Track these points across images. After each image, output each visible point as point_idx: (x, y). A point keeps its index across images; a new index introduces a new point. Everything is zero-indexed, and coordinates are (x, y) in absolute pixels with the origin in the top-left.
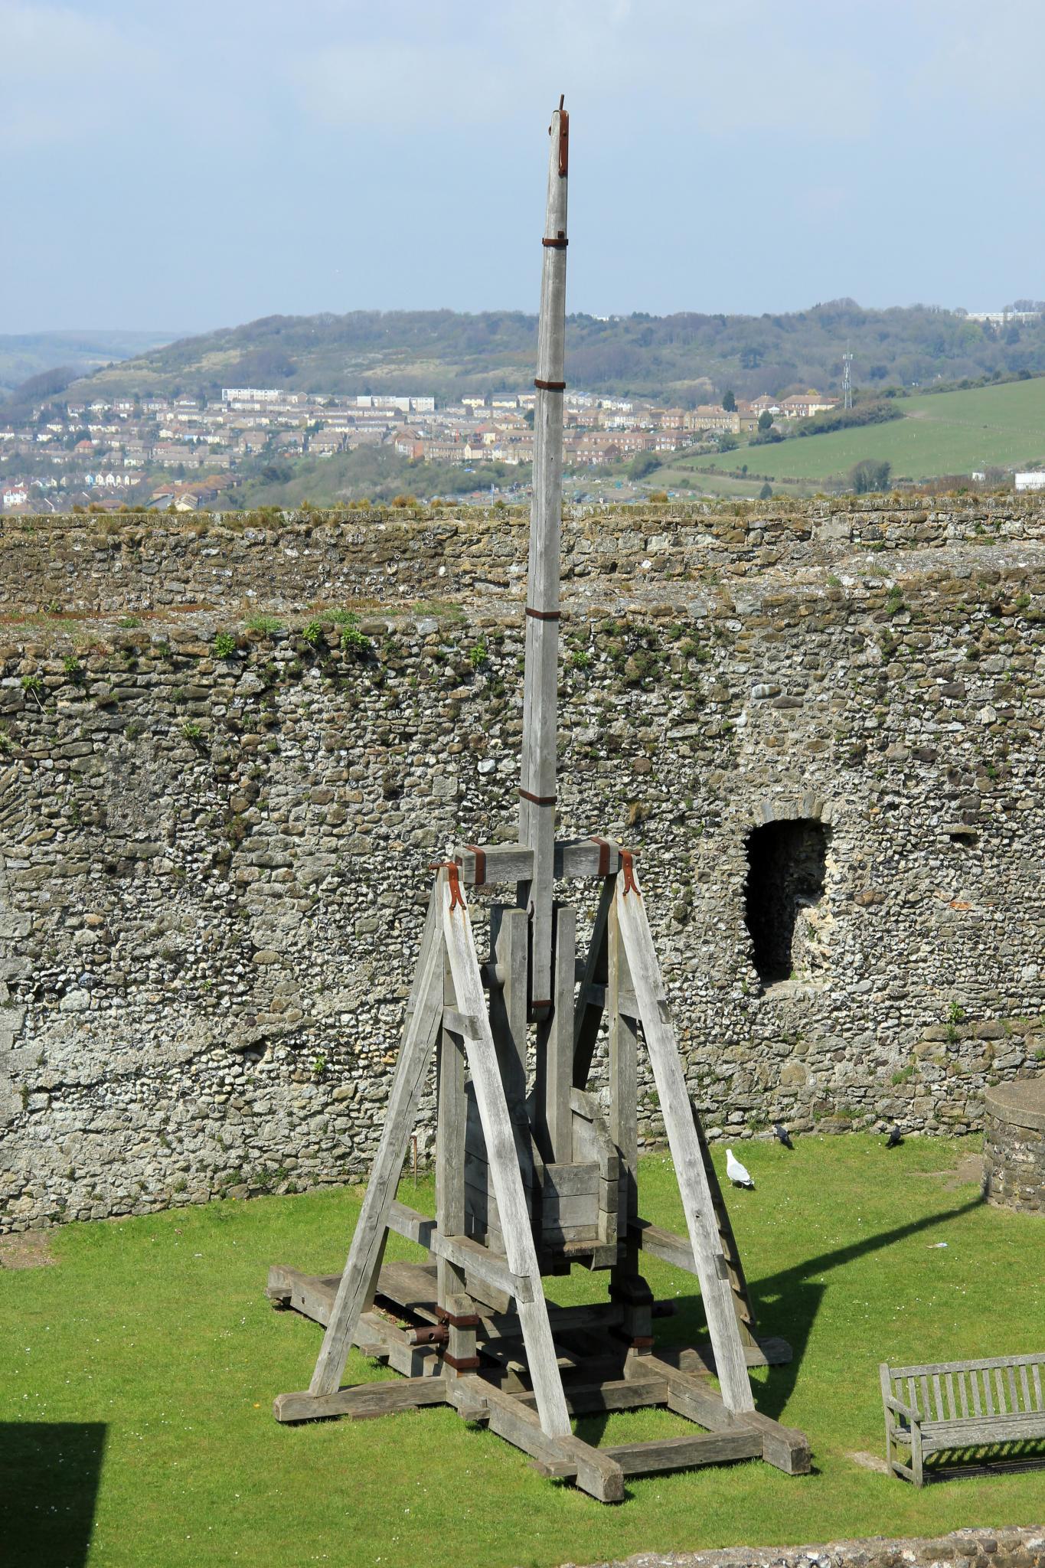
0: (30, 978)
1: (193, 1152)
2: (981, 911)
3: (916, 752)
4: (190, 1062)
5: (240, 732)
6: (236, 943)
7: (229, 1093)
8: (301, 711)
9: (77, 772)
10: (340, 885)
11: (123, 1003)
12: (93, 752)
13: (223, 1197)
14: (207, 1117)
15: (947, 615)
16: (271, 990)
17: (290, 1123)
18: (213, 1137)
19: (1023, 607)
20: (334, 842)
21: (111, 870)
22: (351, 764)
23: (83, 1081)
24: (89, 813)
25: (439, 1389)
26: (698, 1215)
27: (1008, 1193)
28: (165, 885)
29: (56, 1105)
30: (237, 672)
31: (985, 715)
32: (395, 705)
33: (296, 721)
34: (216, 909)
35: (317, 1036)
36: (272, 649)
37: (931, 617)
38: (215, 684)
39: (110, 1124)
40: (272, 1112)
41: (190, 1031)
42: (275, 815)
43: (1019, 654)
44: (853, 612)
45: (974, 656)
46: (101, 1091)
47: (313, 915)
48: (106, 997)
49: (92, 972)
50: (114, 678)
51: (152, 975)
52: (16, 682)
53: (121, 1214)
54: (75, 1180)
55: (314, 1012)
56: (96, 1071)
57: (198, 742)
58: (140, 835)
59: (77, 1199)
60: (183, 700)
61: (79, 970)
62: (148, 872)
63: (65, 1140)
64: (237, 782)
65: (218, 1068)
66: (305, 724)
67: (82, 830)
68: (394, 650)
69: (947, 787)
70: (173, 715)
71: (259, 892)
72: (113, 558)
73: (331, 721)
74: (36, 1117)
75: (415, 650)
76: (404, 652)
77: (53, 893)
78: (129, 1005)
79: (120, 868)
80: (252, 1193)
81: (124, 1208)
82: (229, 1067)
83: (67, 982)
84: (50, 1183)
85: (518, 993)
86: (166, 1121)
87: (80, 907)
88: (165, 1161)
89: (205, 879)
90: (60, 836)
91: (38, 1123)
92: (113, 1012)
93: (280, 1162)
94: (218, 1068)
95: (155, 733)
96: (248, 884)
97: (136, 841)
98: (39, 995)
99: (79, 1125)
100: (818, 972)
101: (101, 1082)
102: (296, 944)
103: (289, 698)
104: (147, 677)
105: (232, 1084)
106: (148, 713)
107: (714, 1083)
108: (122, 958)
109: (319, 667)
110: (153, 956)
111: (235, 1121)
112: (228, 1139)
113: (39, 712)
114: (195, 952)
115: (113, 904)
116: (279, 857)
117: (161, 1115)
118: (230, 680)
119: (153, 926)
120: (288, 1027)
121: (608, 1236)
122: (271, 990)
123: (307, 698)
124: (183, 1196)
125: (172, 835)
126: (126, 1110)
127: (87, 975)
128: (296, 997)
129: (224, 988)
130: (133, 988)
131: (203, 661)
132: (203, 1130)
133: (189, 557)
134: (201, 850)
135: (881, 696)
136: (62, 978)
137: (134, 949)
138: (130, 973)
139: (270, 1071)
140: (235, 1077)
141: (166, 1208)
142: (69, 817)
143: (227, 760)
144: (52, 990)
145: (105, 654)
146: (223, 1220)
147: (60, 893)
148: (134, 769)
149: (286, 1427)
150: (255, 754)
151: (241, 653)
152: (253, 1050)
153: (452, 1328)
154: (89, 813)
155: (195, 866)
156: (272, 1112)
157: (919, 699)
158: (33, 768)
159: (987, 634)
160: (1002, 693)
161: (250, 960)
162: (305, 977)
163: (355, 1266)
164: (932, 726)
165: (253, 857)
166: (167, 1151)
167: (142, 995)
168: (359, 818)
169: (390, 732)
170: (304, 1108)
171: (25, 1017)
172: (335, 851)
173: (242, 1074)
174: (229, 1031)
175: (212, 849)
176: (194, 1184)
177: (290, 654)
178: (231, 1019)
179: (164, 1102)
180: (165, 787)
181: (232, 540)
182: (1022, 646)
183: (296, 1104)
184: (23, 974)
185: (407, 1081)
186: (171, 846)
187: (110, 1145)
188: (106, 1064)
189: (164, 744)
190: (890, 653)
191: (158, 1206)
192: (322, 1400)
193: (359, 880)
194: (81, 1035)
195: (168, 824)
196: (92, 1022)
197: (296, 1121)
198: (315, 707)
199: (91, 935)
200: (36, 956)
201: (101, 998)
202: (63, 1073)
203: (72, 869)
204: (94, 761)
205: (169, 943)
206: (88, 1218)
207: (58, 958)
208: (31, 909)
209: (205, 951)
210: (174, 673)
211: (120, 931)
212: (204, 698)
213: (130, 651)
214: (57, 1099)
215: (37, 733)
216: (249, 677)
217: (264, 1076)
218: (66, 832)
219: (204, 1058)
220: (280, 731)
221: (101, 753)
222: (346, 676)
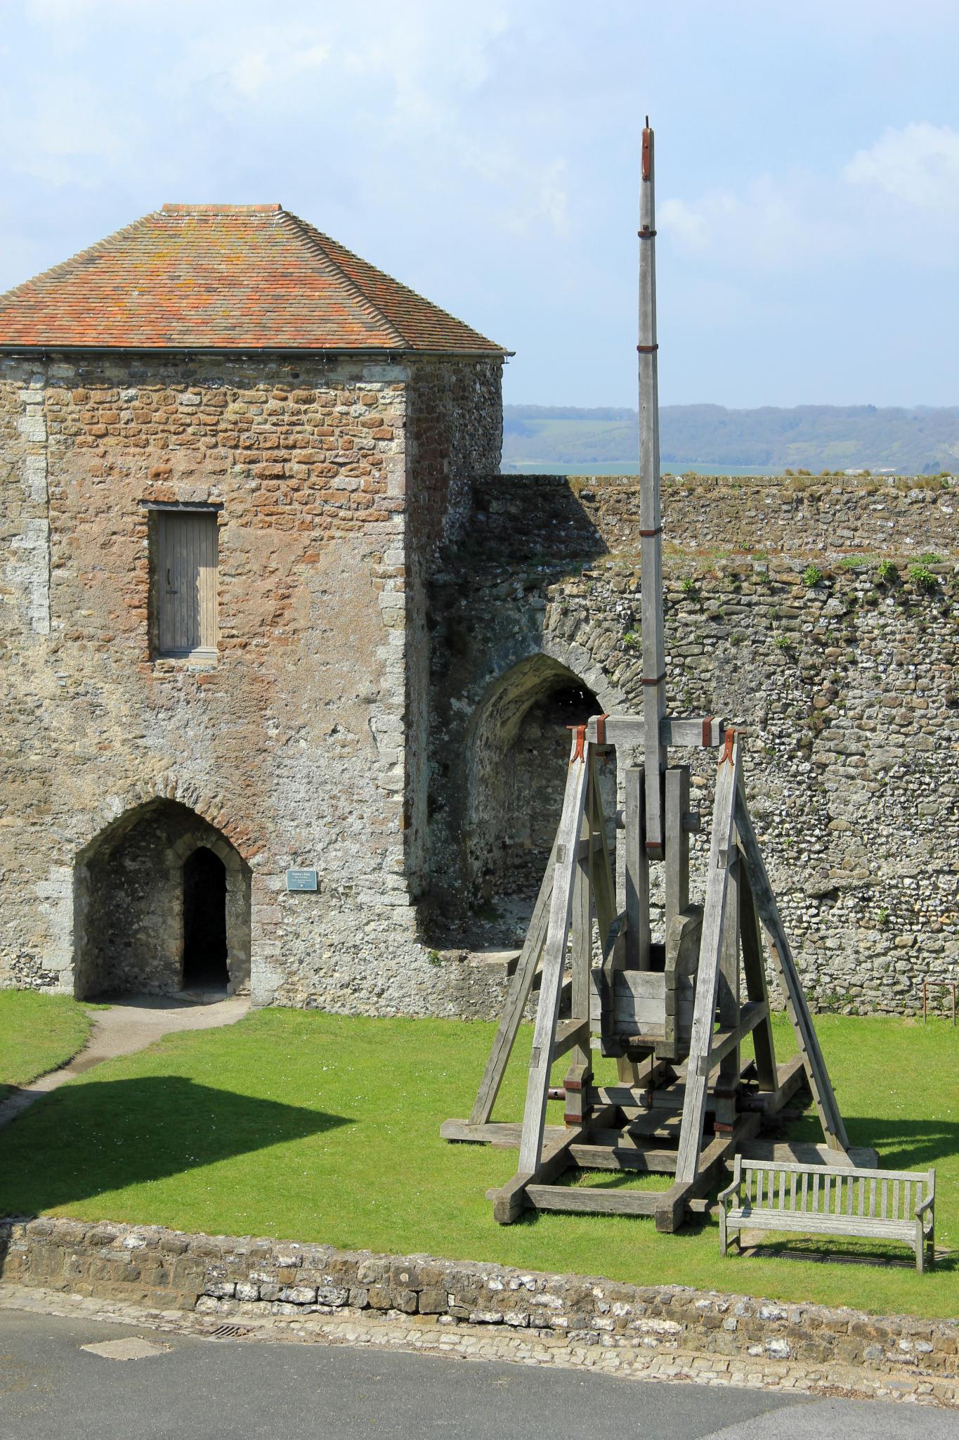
5: (825, 645)
6: (815, 811)
7: (807, 928)
8: (876, 632)
10: (905, 774)
12: (703, 653)
17: (857, 959)
20: (901, 739)
22: (917, 678)
28: (757, 760)
34: (799, 783)
36: (853, 581)
38: (805, 607)
40: (841, 948)
42: (851, 713)
47: (882, 796)
57: (787, 649)
58: (739, 720)
60: (778, 617)
64: (820, 684)
67: (692, 711)
70: (770, 628)
71: (835, 773)
72: (797, 509)
73: (903, 641)
82: (808, 908)
89: (791, 758)
93: (847, 989)
96: (826, 766)
102: (865, 817)
103: (866, 621)
104: (748, 598)
106: (748, 627)
109: (893, 597)
111: (810, 951)
114: (780, 815)
116: (853, 747)
118: (818, 604)
120: (856, 883)
123: (882, 622)
125: (764, 722)
128: (864, 860)
131: (795, 588)
133: (859, 511)
134: (789, 736)
142: (683, 701)
143: (813, 667)
145: (716, 578)
150: (836, 664)
151: (827, 583)
152: (831, 895)
155: (782, 747)
168: (924, 721)
170: (869, 949)
172: (902, 746)
173: (817, 915)
175: (796, 735)
178: (809, 870)
180: (761, 684)
181: (896, 498)
183: (862, 945)
189: (761, 650)
193: (923, 772)
195: (761, 713)
197: (862, 959)
198: (888, 629)
204: (704, 660)
205: (759, 806)
209: (788, 815)
212: (796, 617)
213: (735, 577)
216: (833, 602)
217: (835, 919)
219: (786, 898)
220: (858, 646)
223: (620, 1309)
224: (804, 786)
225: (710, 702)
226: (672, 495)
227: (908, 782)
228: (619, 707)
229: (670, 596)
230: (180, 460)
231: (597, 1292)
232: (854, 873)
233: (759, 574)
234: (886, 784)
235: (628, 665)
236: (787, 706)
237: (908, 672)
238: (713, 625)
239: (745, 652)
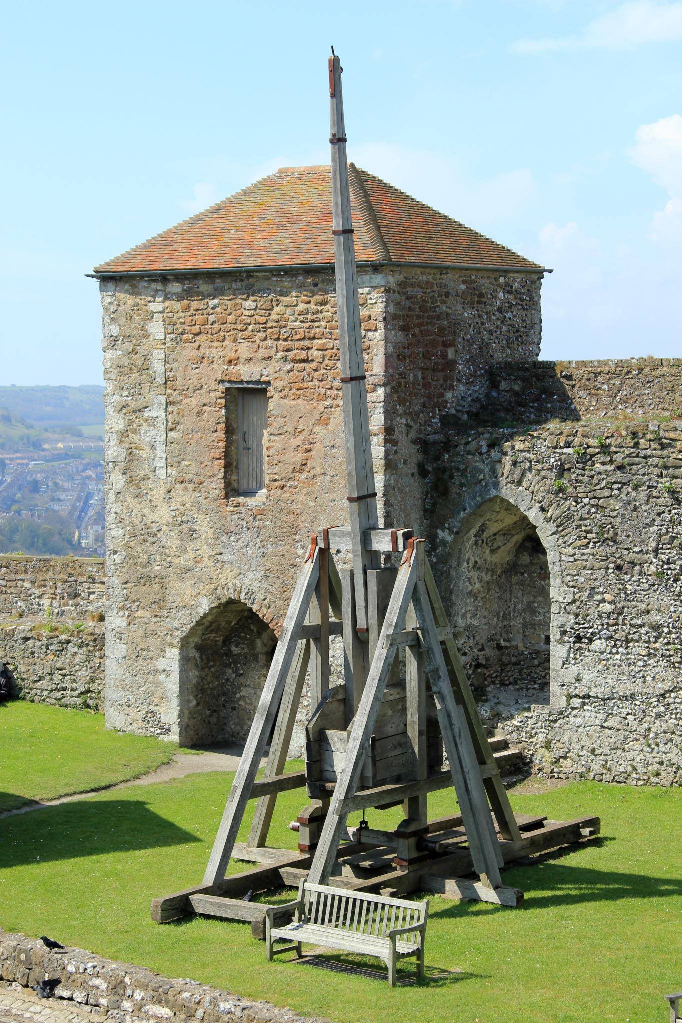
1: (665, 753)
9: (602, 507)
11: (624, 652)
12: (611, 496)
21: (618, 568)
49: (607, 629)
53: (620, 782)
58: (637, 549)
59: (596, 767)
60: (666, 467)
61: (600, 627)
67: (604, 542)
70: (660, 476)
74: (574, 712)
78: (628, 654)
81: (621, 779)
86: (649, 729)
87: (601, 589)
88: (648, 755)
92: (618, 657)
95: (649, 487)
98: (578, 639)
104: (644, 451)
106: (644, 474)
108: (624, 624)
113: (583, 469)
114: (668, 627)
115: (619, 589)
117: (645, 726)
119: (643, 607)
125: (656, 551)
127: (604, 632)
136: (590, 631)
138: (629, 633)
145: (621, 436)
148: (635, 509)
155: (669, 572)
158: (577, 503)
166: (649, 750)
167: (638, 649)
176: (663, 774)
180: (654, 521)
184: (568, 626)
189: (654, 494)
191: (641, 783)
194: (600, 667)
195: (653, 545)
200: (577, 616)
204: (612, 501)
205: (652, 619)
206: (600, 780)
207: (588, 618)
208: (573, 587)
213: (634, 434)
218: (595, 543)
219: (672, 695)
223: (139, 995)
225: (616, 534)
228: (551, 538)
230: (244, 350)
231: (127, 980)
233: (652, 432)
235: (558, 505)
239: (642, 494)
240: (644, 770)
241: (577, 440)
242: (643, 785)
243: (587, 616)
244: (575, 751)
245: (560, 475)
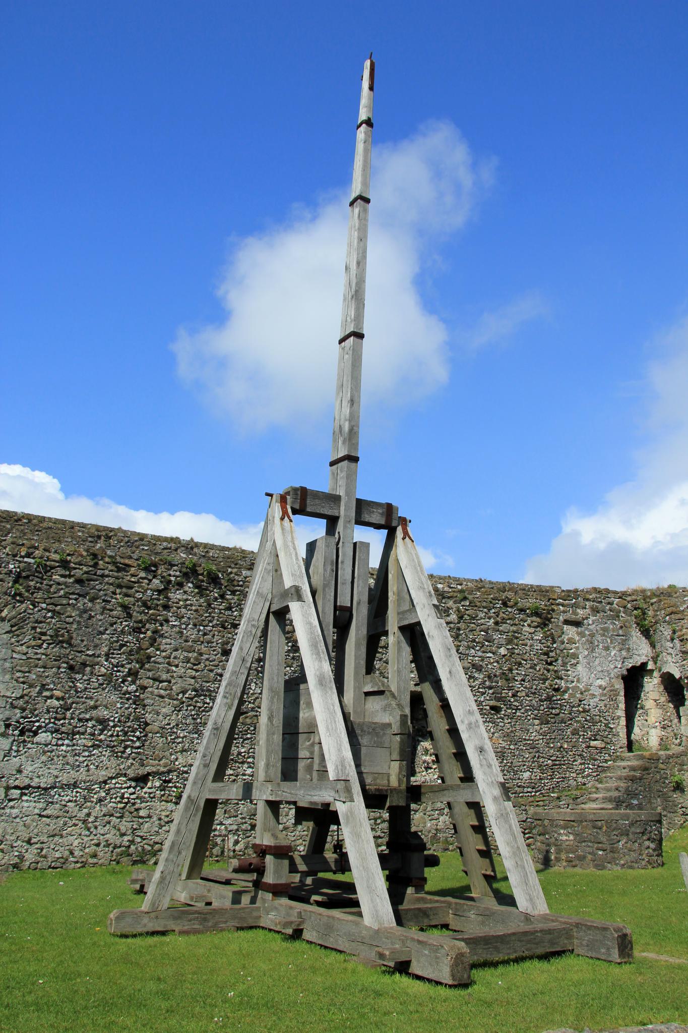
0: (18, 722)
1: (103, 835)
2: (504, 744)
3: (473, 665)
4: (105, 782)
5: (149, 608)
6: (137, 719)
7: (126, 803)
8: (181, 603)
9: (58, 613)
10: (195, 696)
11: (71, 743)
13: (118, 863)
14: (112, 815)
15: (484, 604)
16: (154, 747)
17: (160, 824)
18: (115, 827)
19: (516, 604)
20: (194, 673)
21: (71, 668)
22: (205, 634)
23: (42, 785)
24: (63, 635)
25: (255, 914)
26: (481, 750)
27: (558, 859)
28: (101, 682)
29: (25, 798)
30: (150, 577)
31: (503, 651)
32: (229, 608)
33: (179, 608)
34: (128, 699)
35: (178, 777)
36: (169, 570)
37: (478, 604)
38: (138, 582)
39: (55, 813)
40: (149, 817)
41: (105, 764)
42: (164, 654)
43: (516, 625)
44: (444, 598)
45: (497, 623)
46: (52, 793)
47: (179, 711)
48: (61, 739)
49: (54, 723)
50: (85, 569)
51: (89, 730)
52: (32, 561)
53: (57, 868)
54: (31, 844)
55: (177, 763)
56: (51, 780)
57: (125, 608)
58: (90, 653)
59: (31, 856)
60: (120, 586)
61: (47, 721)
62: (92, 673)
63: (28, 820)
64: (145, 633)
65: (121, 788)
66: (183, 610)
68: (231, 581)
69: (487, 683)
71: (152, 693)
72: (96, 542)
73: (196, 611)
74: (11, 804)
75: (241, 583)
76: (235, 583)
77: (38, 676)
78: (74, 745)
79: (76, 668)
80: (135, 863)
81: (58, 864)
82: (128, 788)
83: (40, 727)
84: (15, 844)
85: (328, 596)
86: (89, 815)
88: (86, 839)
89: (123, 682)
90: (45, 645)
91: (12, 807)
92: (64, 748)
93: (152, 846)
94: (121, 788)
95: (104, 601)
96: (146, 688)
97: (87, 655)
98: (22, 733)
99: (37, 811)
100: (429, 771)
101: (53, 788)
102: (169, 724)
103: (176, 595)
104: (102, 572)
105: (128, 798)
106: (100, 590)
107: (382, 822)
108: (73, 718)
109: (192, 583)
110: (91, 719)
111: (129, 819)
112: (123, 829)
113: (42, 578)
115: (70, 687)
116: (164, 676)
117: (86, 811)
118: (146, 581)
119: (92, 703)
120: (162, 769)
121: (400, 781)
122: (154, 747)
123: (185, 597)
124: (95, 860)
125: (107, 655)
126: (66, 806)
127: (51, 725)
128: (167, 753)
129: (129, 743)
130: (77, 736)
132: (109, 823)
133: (134, 548)
134: (123, 666)
135: (457, 637)
136: (37, 724)
137: (80, 714)
138: (76, 727)
139: (150, 793)
140: (131, 794)
141: (82, 867)
142: (51, 636)
143: (141, 622)
144: (30, 730)
146: (114, 872)
147: (41, 676)
148: (91, 617)
149: (117, 939)
150: (156, 620)
152: (142, 780)
153: (269, 859)
154: (63, 635)
156: (149, 817)
157: (474, 641)
159: (501, 615)
160: (509, 642)
161: (144, 729)
162: (174, 743)
163: (189, 797)
164: (480, 654)
165: (150, 674)
166: (87, 833)
167: (82, 741)
168: (207, 663)
169: (226, 621)
170: (167, 816)
171: (12, 743)
172: (194, 678)
173: (134, 793)
174: (129, 767)
175: (128, 666)
176: (101, 854)
177: (178, 573)
178: (130, 761)
179: (89, 804)
180: (106, 630)
181: (155, 544)
182: (516, 622)
183: (164, 813)
184: (14, 719)
185: (241, 648)
186: (107, 661)
187: (54, 825)
188: (57, 777)
189: (108, 607)
190: (461, 618)
191: (79, 865)
192: (153, 915)
193: (205, 695)
194: (44, 758)
195: (106, 649)
196: (51, 752)
197: (163, 823)
198: (188, 602)
199: (56, 703)
200: (23, 710)
201: (58, 739)
202: (31, 779)
203: (50, 664)
204: (69, 609)
205: (100, 714)
206: (36, 869)
207: (36, 712)
208: (24, 683)
209: (119, 721)
210: (117, 572)
211: (73, 703)
212: (132, 588)
213: (95, 556)
214: (26, 794)
215: (39, 589)
216: (156, 581)
219: (114, 781)
221: (74, 605)
222: (206, 590)
224: (131, 701)
226: (16, 521)
227: (197, 702)
228: (5, 636)
229: (48, 563)
232: (161, 762)
233: (110, 557)
234: (183, 703)
235: (14, 607)
236: (122, 646)
237: (199, 631)
238: (78, 586)
239: (98, 607)
240: (81, 853)
241: (37, 553)
242: (82, 867)
243: (35, 710)
244: (9, 843)
245: (16, 582)
